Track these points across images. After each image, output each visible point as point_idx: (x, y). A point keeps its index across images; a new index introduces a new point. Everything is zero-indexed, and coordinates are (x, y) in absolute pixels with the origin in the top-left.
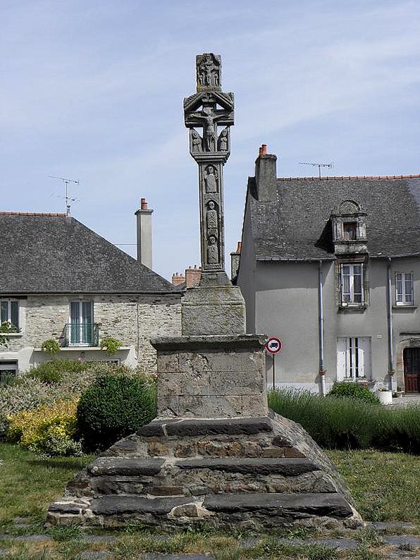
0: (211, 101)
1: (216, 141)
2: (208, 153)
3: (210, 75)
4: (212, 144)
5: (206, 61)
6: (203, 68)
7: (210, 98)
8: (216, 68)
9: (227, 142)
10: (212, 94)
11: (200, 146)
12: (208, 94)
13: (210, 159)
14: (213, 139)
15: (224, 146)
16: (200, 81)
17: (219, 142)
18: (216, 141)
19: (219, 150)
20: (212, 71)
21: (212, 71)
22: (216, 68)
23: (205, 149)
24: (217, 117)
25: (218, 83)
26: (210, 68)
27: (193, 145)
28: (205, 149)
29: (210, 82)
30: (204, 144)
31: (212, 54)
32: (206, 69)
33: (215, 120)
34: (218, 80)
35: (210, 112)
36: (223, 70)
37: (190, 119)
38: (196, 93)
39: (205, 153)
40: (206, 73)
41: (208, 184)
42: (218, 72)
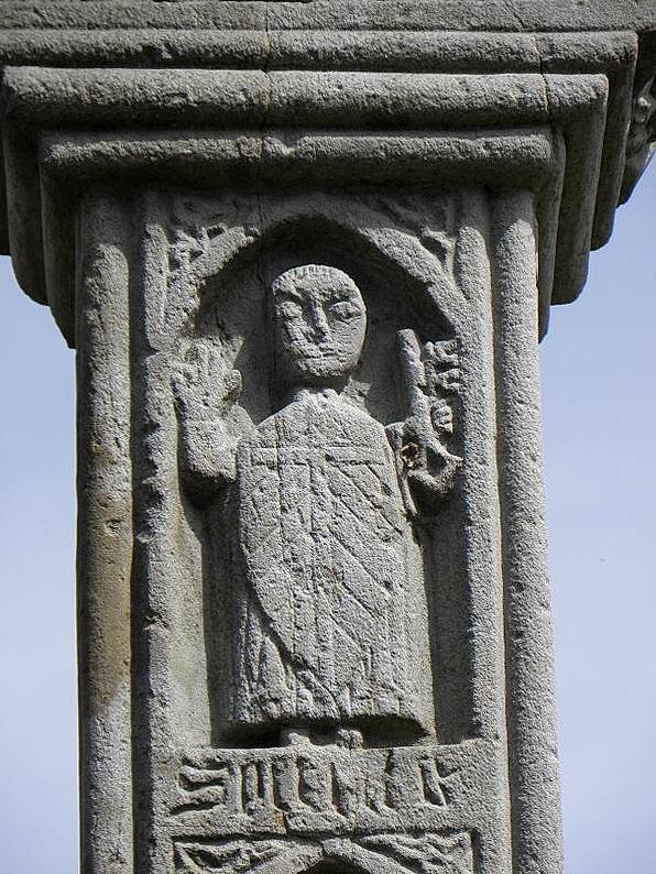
13: (299, 116)
41: (273, 578)
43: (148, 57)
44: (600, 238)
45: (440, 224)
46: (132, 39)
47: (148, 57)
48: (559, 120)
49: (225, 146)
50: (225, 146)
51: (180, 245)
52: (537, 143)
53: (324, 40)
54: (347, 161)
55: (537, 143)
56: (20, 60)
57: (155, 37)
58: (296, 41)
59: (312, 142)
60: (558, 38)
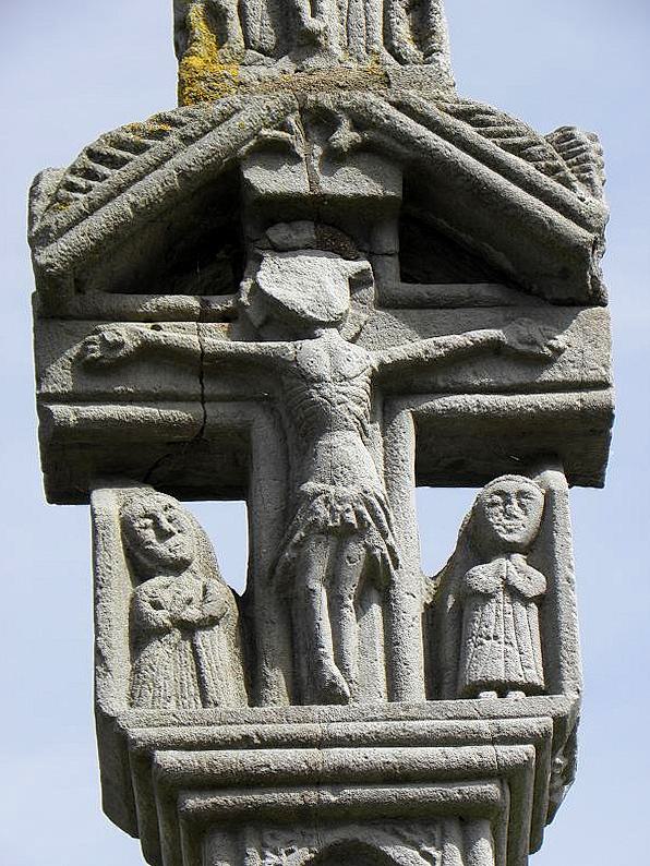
0: (352, 183)
1: (412, 595)
2: (318, 719)
4: (362, 634)
9: (547, 604)
10: (361, 120)
11: (220, 648)
12: (320, 121)
13: (341, 777)
14: (378, 583)
19: (445, 679)
23: (277, 678)
24: (410, 345)
25: (424, 33)
27: (142, 634)
28: (277, 678)
30: (273, 639)
35: (341, 299)
38: (168, 104)
39: (279, 712)
43: (246, 742)
44: (535, 846)
45: (432, 843)
46: (235, 731)
47: (246, 742)
48: (504, 775)
49: (295, 797)
50: (295, 797)
51: (268, 860)
52: (491, 789)
53: (355, 728)
54: (373, 804)
55: (491, 789)
56: (165, 747)
57: (249, 729)
58: (338, 729)
59: (349, 792)
60: (503, 723)
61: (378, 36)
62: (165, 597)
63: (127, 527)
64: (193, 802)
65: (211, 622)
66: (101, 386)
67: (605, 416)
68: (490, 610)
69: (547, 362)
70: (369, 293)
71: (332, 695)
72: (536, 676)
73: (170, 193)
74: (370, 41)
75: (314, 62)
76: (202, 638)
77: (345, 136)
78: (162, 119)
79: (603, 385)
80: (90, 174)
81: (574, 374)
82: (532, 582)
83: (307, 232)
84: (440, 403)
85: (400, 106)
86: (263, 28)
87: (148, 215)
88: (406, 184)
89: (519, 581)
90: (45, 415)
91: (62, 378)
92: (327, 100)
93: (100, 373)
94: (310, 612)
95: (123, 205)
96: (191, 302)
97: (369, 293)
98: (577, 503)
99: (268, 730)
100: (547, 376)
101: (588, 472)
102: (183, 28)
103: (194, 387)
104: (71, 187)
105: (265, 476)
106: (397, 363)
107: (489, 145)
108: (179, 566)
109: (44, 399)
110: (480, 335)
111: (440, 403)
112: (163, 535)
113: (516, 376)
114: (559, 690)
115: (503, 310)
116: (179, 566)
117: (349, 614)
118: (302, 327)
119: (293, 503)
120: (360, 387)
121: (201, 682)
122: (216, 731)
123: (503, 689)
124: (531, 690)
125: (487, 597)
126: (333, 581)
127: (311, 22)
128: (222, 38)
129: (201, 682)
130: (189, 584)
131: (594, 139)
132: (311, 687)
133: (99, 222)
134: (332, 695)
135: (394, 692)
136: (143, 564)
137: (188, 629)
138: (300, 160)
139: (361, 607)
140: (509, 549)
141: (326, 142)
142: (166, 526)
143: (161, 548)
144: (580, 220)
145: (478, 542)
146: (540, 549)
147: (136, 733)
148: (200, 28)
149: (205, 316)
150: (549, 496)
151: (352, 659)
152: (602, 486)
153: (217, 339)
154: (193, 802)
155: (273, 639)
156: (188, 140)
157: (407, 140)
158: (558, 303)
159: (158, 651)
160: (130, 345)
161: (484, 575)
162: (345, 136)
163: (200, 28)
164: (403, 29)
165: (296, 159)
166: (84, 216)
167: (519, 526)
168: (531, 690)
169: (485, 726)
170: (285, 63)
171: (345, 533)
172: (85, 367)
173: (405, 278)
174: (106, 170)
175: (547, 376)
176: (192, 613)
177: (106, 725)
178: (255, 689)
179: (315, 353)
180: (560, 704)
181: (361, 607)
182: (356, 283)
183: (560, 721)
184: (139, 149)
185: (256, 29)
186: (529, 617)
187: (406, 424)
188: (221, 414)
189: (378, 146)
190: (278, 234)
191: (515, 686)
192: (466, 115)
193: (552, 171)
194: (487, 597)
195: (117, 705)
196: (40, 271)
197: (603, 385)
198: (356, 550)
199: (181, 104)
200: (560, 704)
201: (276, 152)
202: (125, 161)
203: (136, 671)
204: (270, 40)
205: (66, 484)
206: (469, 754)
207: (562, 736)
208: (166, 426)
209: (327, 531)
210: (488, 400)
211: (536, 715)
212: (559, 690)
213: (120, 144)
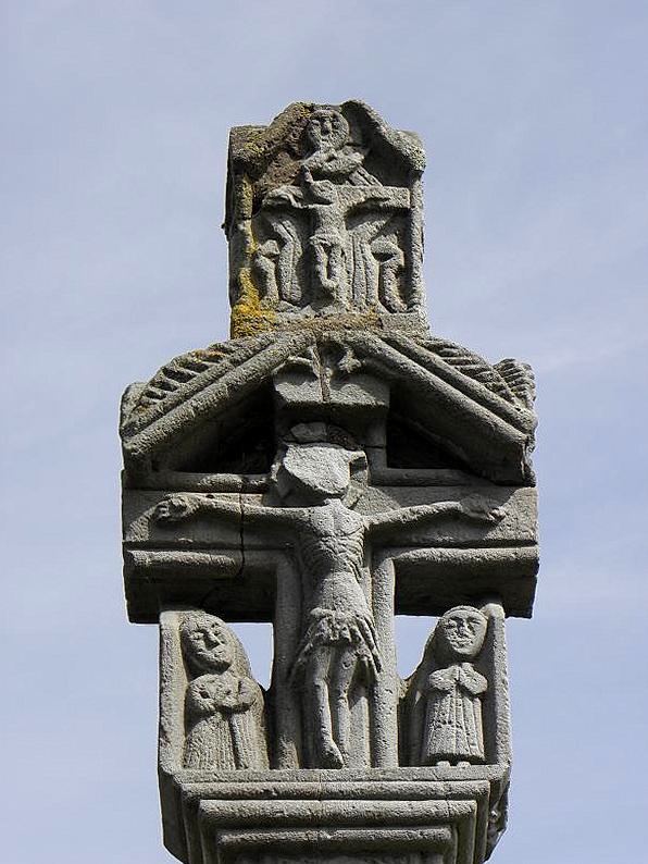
0: (353, 395)
2: (320, 779)
3: (335, 232)
5: (310, 147)
6: (286, 191)
7: (341, 378)
8: (393, 195)
9: (488, 699)
10: (360, 352)
11: (250, 727)
12: (331, 351)
13: (335, 821)
14: (365, 682)
15: (458, 727)
16: (259, 276)
17: (418, 710)
18: (390, 698)
19: (413, 750)
20: (355, 215)
21: (355, 215)
22: (393, 195)
23: (290, 749)
24: (393, 512)
25: (407, 291)
26: (337, 201)
27: (193, 715)
28: (290, 749)
29: (338, 280)
30: (288, 721)
31: (355, 112)
32: (310, 196)
33: (379, 541)
34: (406, 274)
35: (343, 478)
36: (430, 202)
37: (169, 528)
38: (222, 336)
39: (291, 774)
40: (309, 222)
42: (400, 221)
43: (266, 795)
46: (259, 787)
47: (266, 795)
48: (454, 822)
49: (301, 835)
50: (301, 835)
51: (213, 701)
52: (444, 832)
53: (346, 786)
54: (358, 841)
55: (444, 832)
56: (208, 797)
58: (334, 786)
59: (341, 833)
61: (375, 292)
62: (211, 689)
63: (184, 637)
64: (226, 838)
65: (244, 708)
66: (169, 537)
67: (533, 565)
68: (447, 702)
69: (491, 525)
70: (365, 474)
71: (330, 762)
72: (478, 750)
73: (222, 401)
74: (368, 295)
75: (328, 310)
76: (237, 719)
77: (349, 362)
78: (218, 348)
79: (532, 543)
80: (164, 386)
81: (511, 534)
82: (478, 683)
83: (320, 430)
84: (412, 554)
85: (389, 341)
86: (292, 286)
87: (206, 416)
88: (392, 398)
89: (467, 682)
90: (128, 558)
91: (141, 531)
92: (337, 336)
93: (169, 528)
94: (316, 703)
95: (187, 408)
96: (236, 479)
97: (365, 474)
98: (512, 629)
99: (282, 786)
100: (491, 535)
101: (520, 605)
102: (235, 285)
103: (235, 539)
104: (151, 395)
105: (286, 606)
106: (382, 525)
107: (452, 370)
108: (221, 667)
109: (127, 546)
110: (442, 505)
111: (412, 554)
112: (211, 645)
113: (469, 535)
114: (495, 761)
115: (461, 488)
116: (221, 667)
117: (344, 704)
118: (315, 497)
119: (305, 623)
120: (356, 540)
121: (235, 751)
122: (245, 786)
123: (454, 760)
124: (474, 761)
125: (444, 693)
126: (333, 680)
127: (327, 282)
128: (263, 292)
129: (235, 751)
130: (228, 680)
131: (528, 368)
132: (315, 756)
133: (170, 420)
134: (330, 762)
135: (375, 761)
136: (196, 665)
137: (227, 713)
138: (313, 377)
139: (353, 699)
140: (460, 659)
141: (335, 366)
142: (213, 638)
143: (210, 654)
144: (517, 424)
145: (439, 653)
146: (484, 659)
147: (187, 787)
148: (247, 285)
149: (245, 489)
150: (491, 621)
151: (345, 736)
152: (530, 617)
153: (253, 505)
154: (226, 838)
155: (288, 721)
156: (236, 363)
157: (393, 365)
158: (501, 484)
159: (204, 728)
160: (191, 508)
161: (442, 678)
162: (349, 362)
163: (247, 285)
164: (393, 288)
165: (313, 377)
166: (160, 415)
167: (469, 643)
168: (474, 761)
169: (440, 785)
170: (307, 310)
171: (342, 645)
172: (157, 523)
173: (390, 465)
174: (176, 383)
175: (491, 535)
176: (230, 701)
177: (166, 780)
178: (274, 757)
179: (324, 516)
180: (496, 771)
181: (353, 699)
182: (355, 467)
183: (495, 784)
184: (201, 368)
185: (287, 286)
186: (474, 708)
187: (389, 569)
188: (254, 559)
189: (372, 369)
190: (300, 431)
191: (463, 758)
192: (436, 349)
193: (496, 389)
194: (444, 693)
195: (174, 766)
196: (126, 453)
197: (532, 543)
198: (350, 657)
199: (232, 338)
200: (496, 771)
201: (300, 373)
202: (190, 377)
203: (188, 742)
204: (297, 294)
205: (143, 608)
206: (429, 806)
207: (496, 796)
208: (215, 566)
209: (329, 644)
210: (448, 552)
211: (477, 779)
212: (495, 761)
213: (187, 365)
